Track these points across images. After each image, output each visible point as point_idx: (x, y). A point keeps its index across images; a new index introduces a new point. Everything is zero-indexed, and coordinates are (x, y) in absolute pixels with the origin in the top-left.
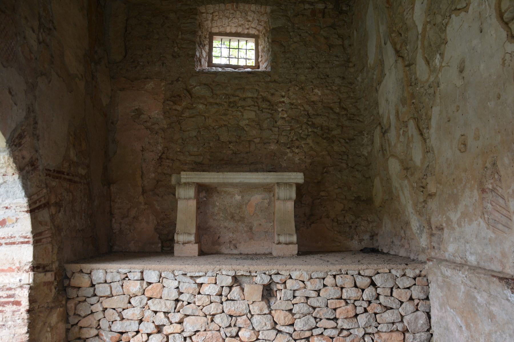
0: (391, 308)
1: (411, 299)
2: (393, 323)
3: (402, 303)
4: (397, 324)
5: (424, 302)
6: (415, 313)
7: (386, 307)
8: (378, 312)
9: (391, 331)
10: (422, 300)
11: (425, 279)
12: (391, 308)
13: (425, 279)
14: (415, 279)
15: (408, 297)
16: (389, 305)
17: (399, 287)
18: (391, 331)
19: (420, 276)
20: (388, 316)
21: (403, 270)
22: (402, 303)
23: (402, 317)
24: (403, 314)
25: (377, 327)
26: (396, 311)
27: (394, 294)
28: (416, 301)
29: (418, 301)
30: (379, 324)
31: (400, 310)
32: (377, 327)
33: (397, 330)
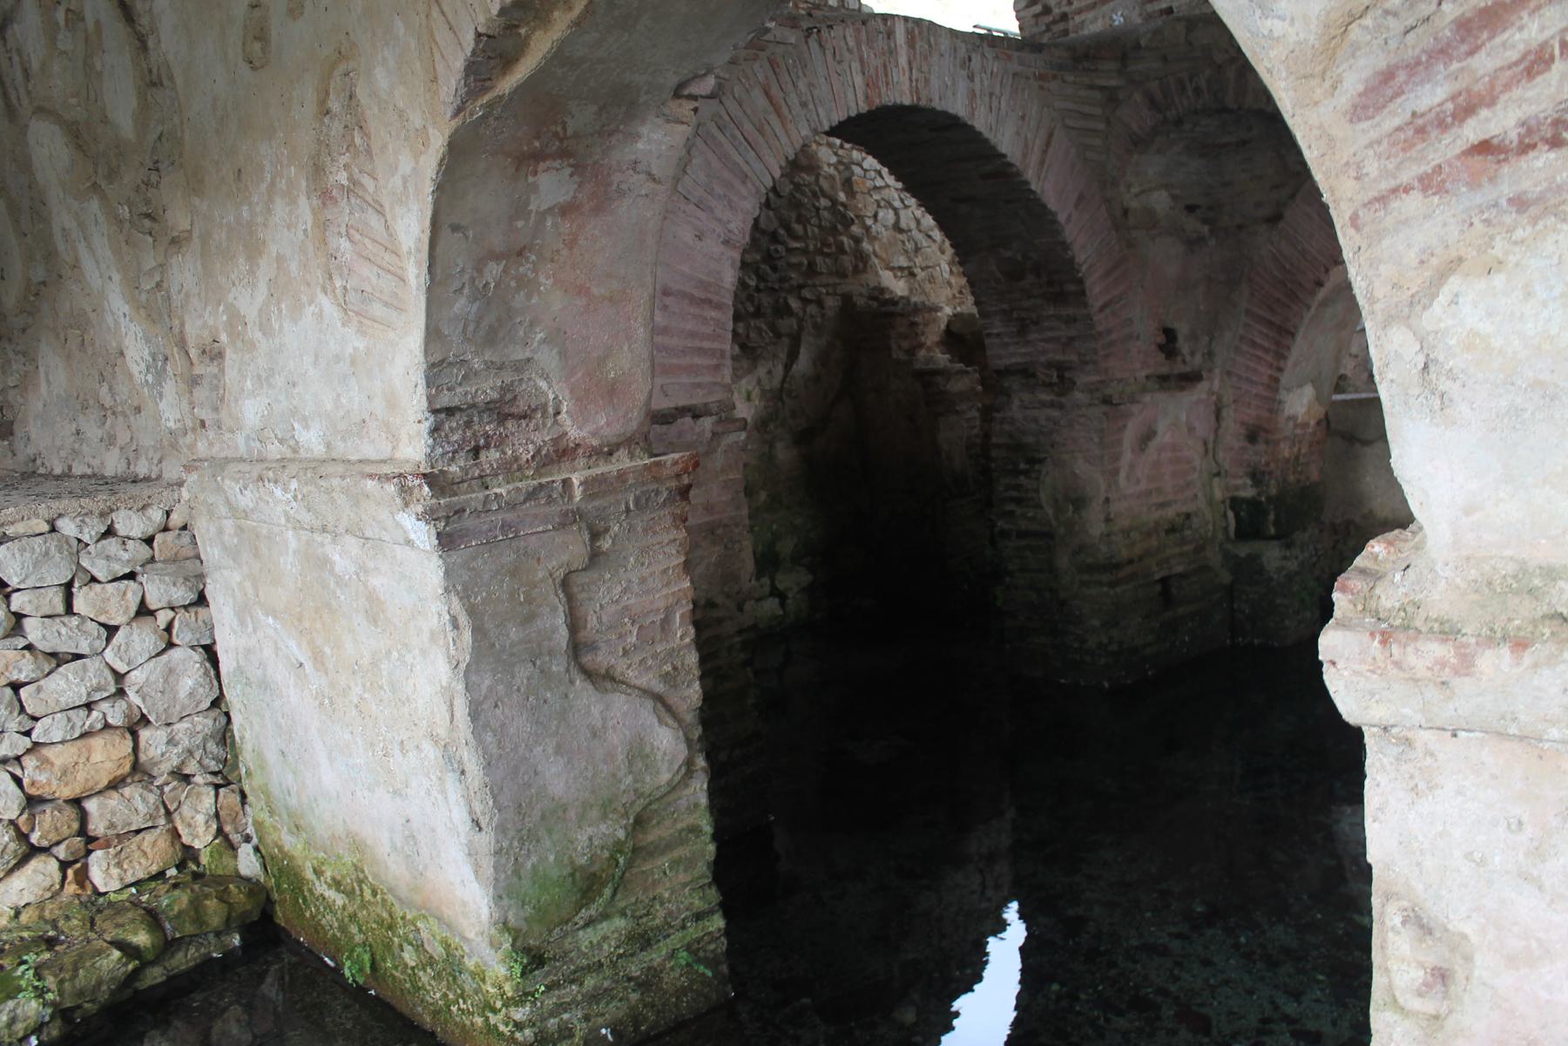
0: (78, 657)
1: (144, 611)
2: (89, 706)
3: (112, 630)
4: (105, 706)
5: (190, 616)
6: (164, 658)
7: (53, 655)
8: (23, 678)
9: (85, 735)
10: (185, 607)
11: (186, 539)
12: (78, 657)
13: (186, 539)
14: (149, 541)
15: (134, 608)
16: (65, 647)
17: (94, 580)
18: (85, 735)
19: (166, 529)
20: (67, 685)
21: (102, 515)
22: (112, 630)
23: (119, 677)
24: (122, 668)
25: (28, 734)
26: (93, 665)
27: (79, 604)
28: (163, 618)
29: (171, 614)
30: (35, 719)
31: (109, 655)
32: (28, 734)
33: (107, 726)
